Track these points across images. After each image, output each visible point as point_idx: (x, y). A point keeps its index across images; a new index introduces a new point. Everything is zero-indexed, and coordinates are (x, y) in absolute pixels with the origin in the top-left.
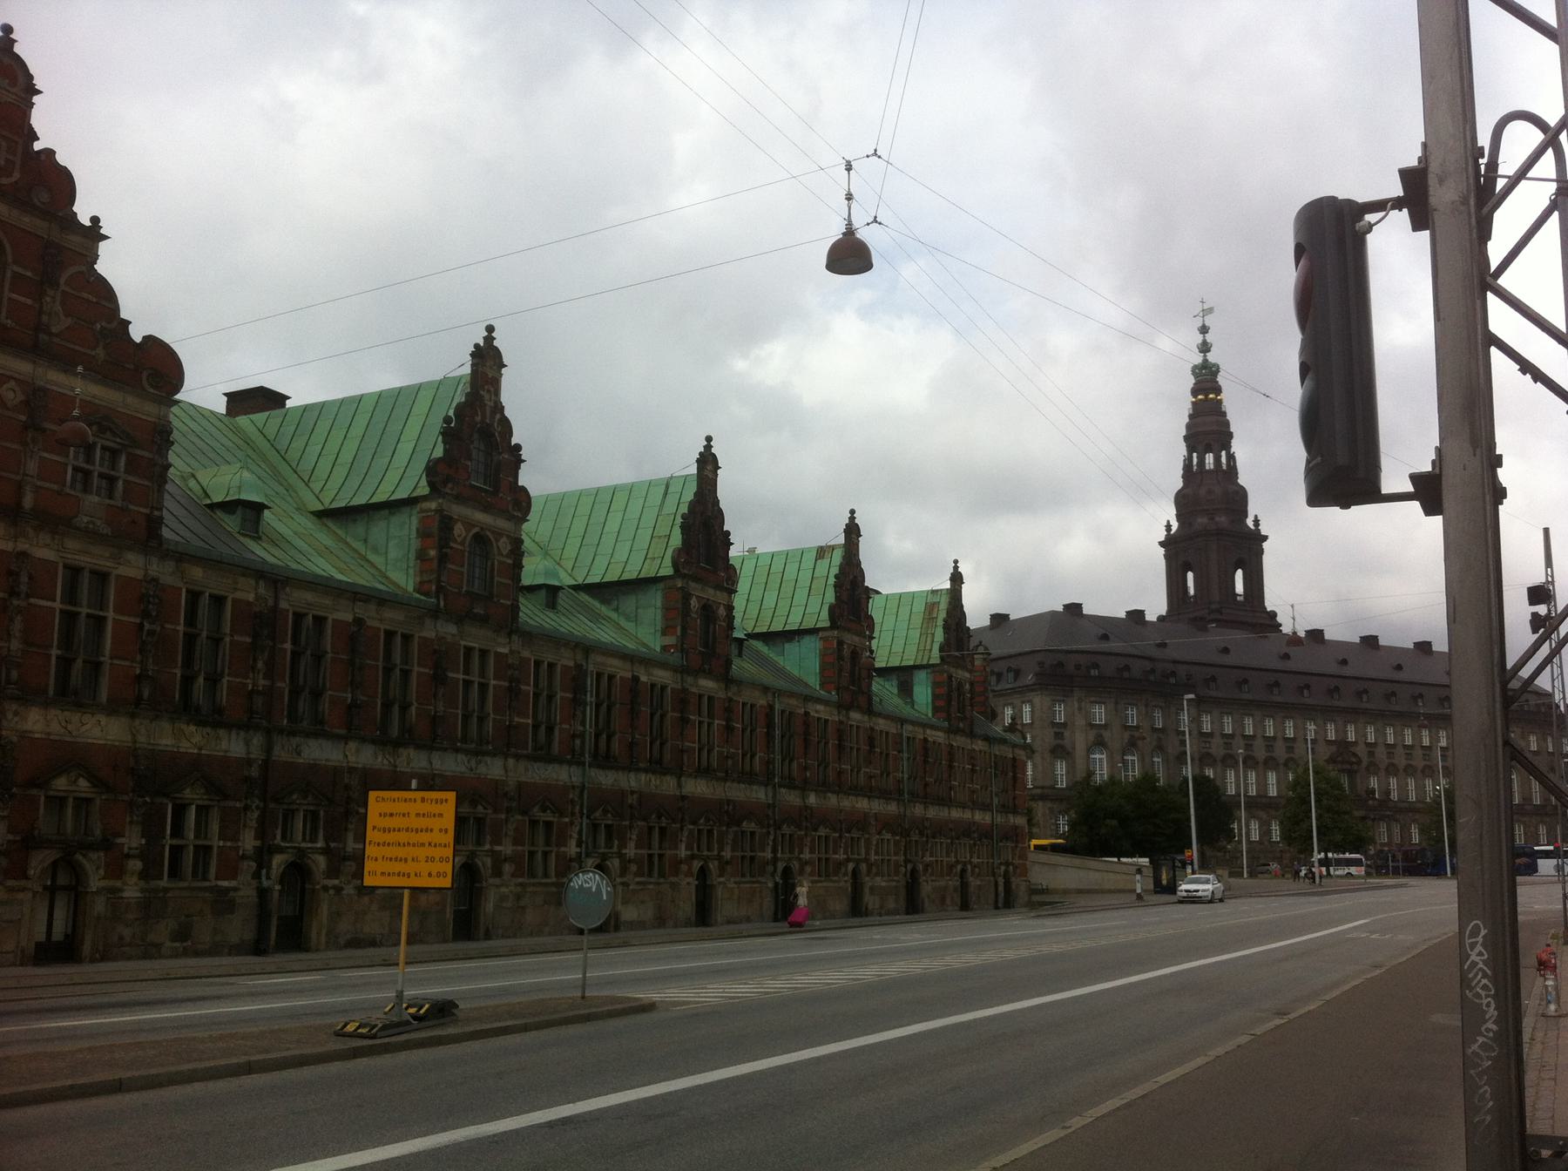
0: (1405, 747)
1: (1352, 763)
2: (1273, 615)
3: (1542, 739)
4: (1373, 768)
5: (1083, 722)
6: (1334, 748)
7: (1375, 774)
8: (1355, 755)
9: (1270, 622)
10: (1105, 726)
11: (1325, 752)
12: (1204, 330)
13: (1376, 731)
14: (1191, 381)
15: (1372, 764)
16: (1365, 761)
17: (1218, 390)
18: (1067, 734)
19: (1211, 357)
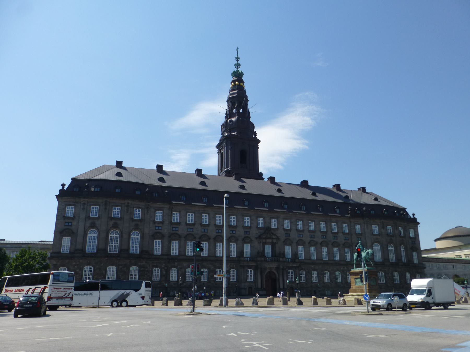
0: (310, 232)
1: (273, 239)
2: (261, 174)
3: (396, 227)
4: (288, 241)
5: (84, 216)
6: (262, 231)
7: (289, 244)
8: (275, 235)
9: (259, 176)
10: (98, 218)
11: (254, 233)
12: (238, 59)
13: (291, 223)
14: (231, 79)
15: (286, 239)
16: (283, 238)
17: (243, 82)
18: (74, 223)
19: (240, 70)
